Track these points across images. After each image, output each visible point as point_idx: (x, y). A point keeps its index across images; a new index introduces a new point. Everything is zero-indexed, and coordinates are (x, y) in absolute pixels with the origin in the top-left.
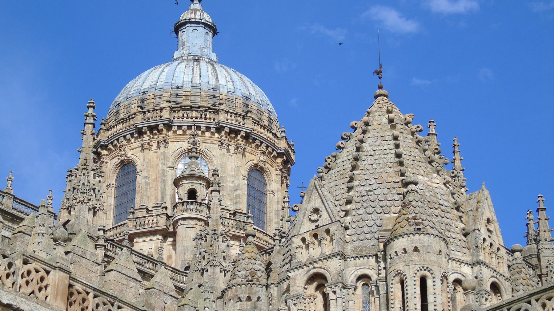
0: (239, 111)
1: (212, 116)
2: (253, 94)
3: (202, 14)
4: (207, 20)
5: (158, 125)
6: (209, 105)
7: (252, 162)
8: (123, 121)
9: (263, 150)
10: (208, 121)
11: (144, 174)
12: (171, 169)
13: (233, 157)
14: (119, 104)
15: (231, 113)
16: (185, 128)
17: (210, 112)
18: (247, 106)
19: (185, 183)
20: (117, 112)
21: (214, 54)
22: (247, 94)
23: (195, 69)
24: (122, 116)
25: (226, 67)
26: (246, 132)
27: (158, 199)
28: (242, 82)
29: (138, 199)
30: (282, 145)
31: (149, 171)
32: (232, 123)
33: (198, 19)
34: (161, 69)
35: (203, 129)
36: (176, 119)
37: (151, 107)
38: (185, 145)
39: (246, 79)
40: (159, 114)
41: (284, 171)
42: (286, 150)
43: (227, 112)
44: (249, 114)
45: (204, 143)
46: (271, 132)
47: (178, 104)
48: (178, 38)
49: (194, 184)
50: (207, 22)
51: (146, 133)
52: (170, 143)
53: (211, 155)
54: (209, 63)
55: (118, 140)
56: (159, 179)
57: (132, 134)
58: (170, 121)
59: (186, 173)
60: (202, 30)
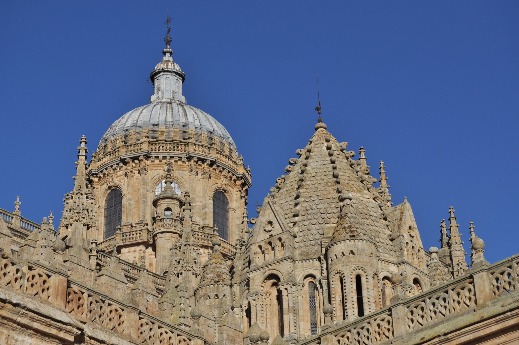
0: (205, 143)
3: (173, 64)
4: (178, 69)
5: (139, 156)
6: (181, 140)
9: (225, 175)
10: (179, 152)
11: (129, 197)
12: (150, 192)
13: (201, 181)
14: (106, 140)
15: (199, 145)
16: (161, 158)
17: (181, 145)
18: (211, 139)
19: (162, 204)
20: (105, 146)
21: (184, 97)
22: (211, 129)
23: (168, 110)
24: (109, 150)
25: (193, 108)
26: (211, 161)
27: (140, 218)
28: (206, 120)
29: (123, 218)
30: (241, 171)
31: (133, 194)
32: (199, 154)
33: (170, 69)
34: (141, 110)
35: (176, 158)
39: (210, 117)
44: (213, 146)
45: (177, 170)
46: (231, 160)
47: (156, 138)
48: (154, 84)
50: (177, 71)
51: (129, 162)
53: (183, 180)
54: (180, 104)
55: (106, 169)
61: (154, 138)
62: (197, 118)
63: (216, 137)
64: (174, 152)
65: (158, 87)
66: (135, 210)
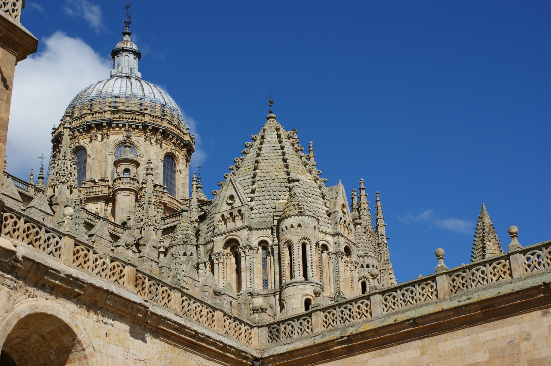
0: (159, 114)
1: (140, 118)
2: (167, 102)
3: (131, 44)
4: (135, 49)
5: (102, 123)
6: (138, 110)
7: (167, 150)
8: (78, 119)
9: (174, 142)
11: (92, 156)
15: (153, 116)
17: (139, 115)
18: (163, 111)
19: (122, 165)
21: (140, 73)
22: (163, 103)
23: (128, 84)
24: (76, 115)
25: (150, 84)
26: (163, 129)
27: (102, 175)
28: (160, 94)
29: (88, 174)
31: (96, 154)
32: (154, 123)
35: (134, 126)
36: (115, 119)
37: (97, 109)
38: (121, 138)
40: (103, 115)
41: (188, 156)
42: (189, 142)
43: (150, 115)
44: (165, 117)
46: (171, 124)
48: (114, 60)
49: (128, 165)
52: (110, 135)
53: (139, 145)
54: (137, 79)
56: (103, 161)
57: (83, 129)
58: (110, 119)
59: (122, 158)
60: (132, 56)
61: (115, 108)
62: (152, 93)
63: (167, 109)
64: (132, 121)
65: (119, 62)
66: (98, 168)
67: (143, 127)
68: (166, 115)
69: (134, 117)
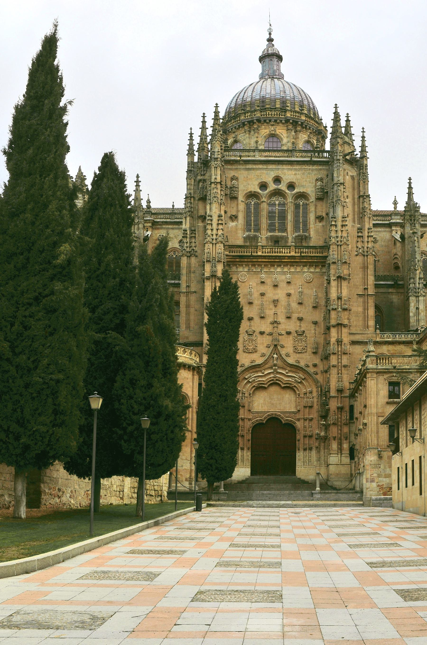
26: (301, 122)
44: (303, 112)
61: (263, 107)
67: (285, 121)
68: (304, 110)
69: (278, 114)
